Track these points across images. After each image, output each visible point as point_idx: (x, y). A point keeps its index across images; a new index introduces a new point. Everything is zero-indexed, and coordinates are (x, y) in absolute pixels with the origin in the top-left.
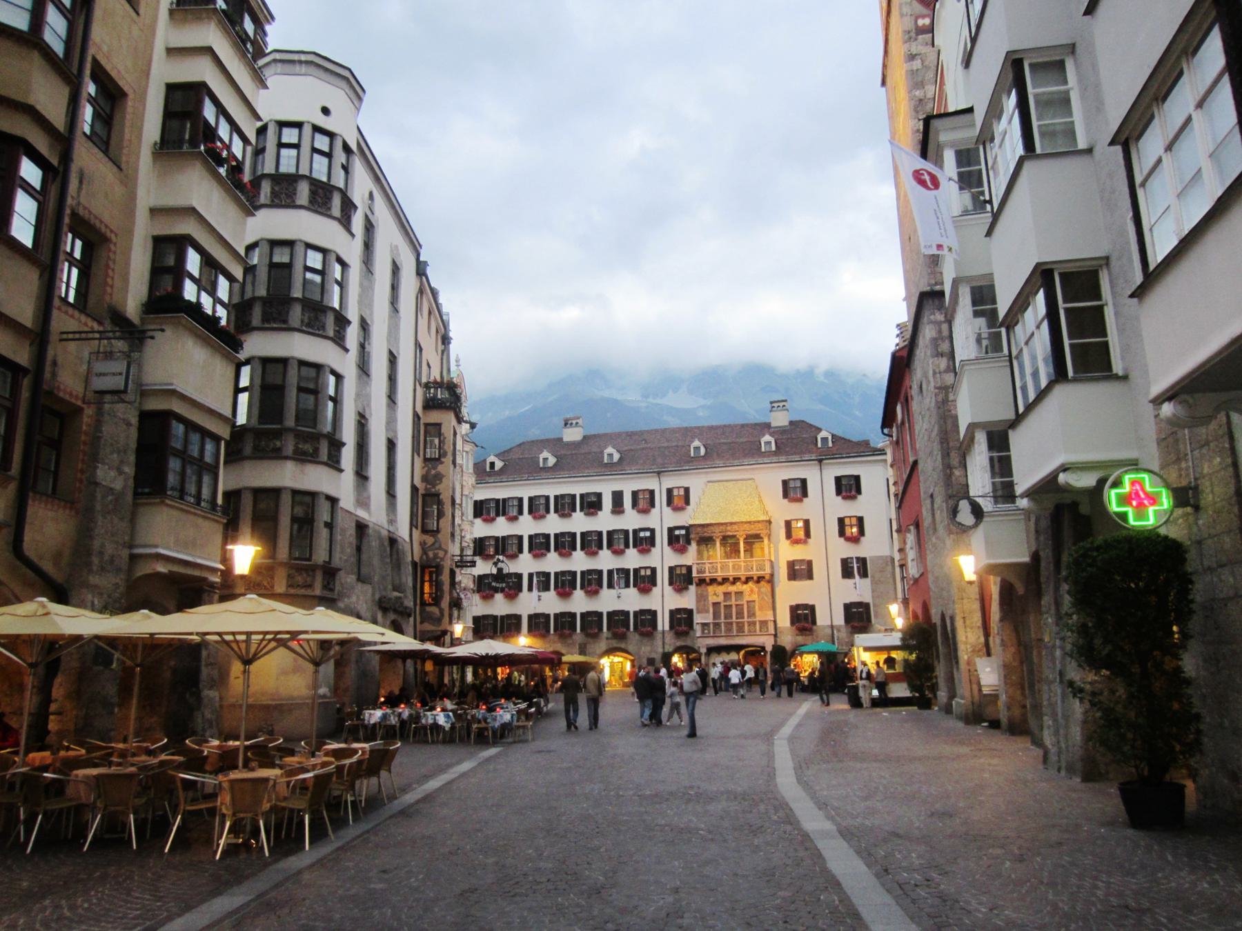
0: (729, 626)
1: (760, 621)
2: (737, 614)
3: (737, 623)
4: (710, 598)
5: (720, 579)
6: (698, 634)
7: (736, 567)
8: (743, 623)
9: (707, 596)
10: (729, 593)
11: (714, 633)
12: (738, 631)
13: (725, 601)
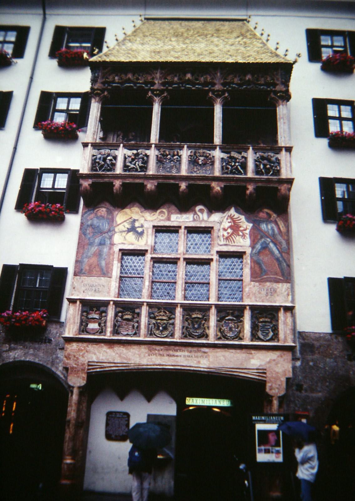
0: (163, 316)
1: (253, 308)
2: (189, 284)
3: (188, 309)
4: (117, 239)
5: (150, 186)
6: (70, 331)
7: (201, 160)
8: (205, 309)
9: (111, 231)
10: (174, 230)
11: (116, 332)
12: (186, 333)
13: (154, 250)
